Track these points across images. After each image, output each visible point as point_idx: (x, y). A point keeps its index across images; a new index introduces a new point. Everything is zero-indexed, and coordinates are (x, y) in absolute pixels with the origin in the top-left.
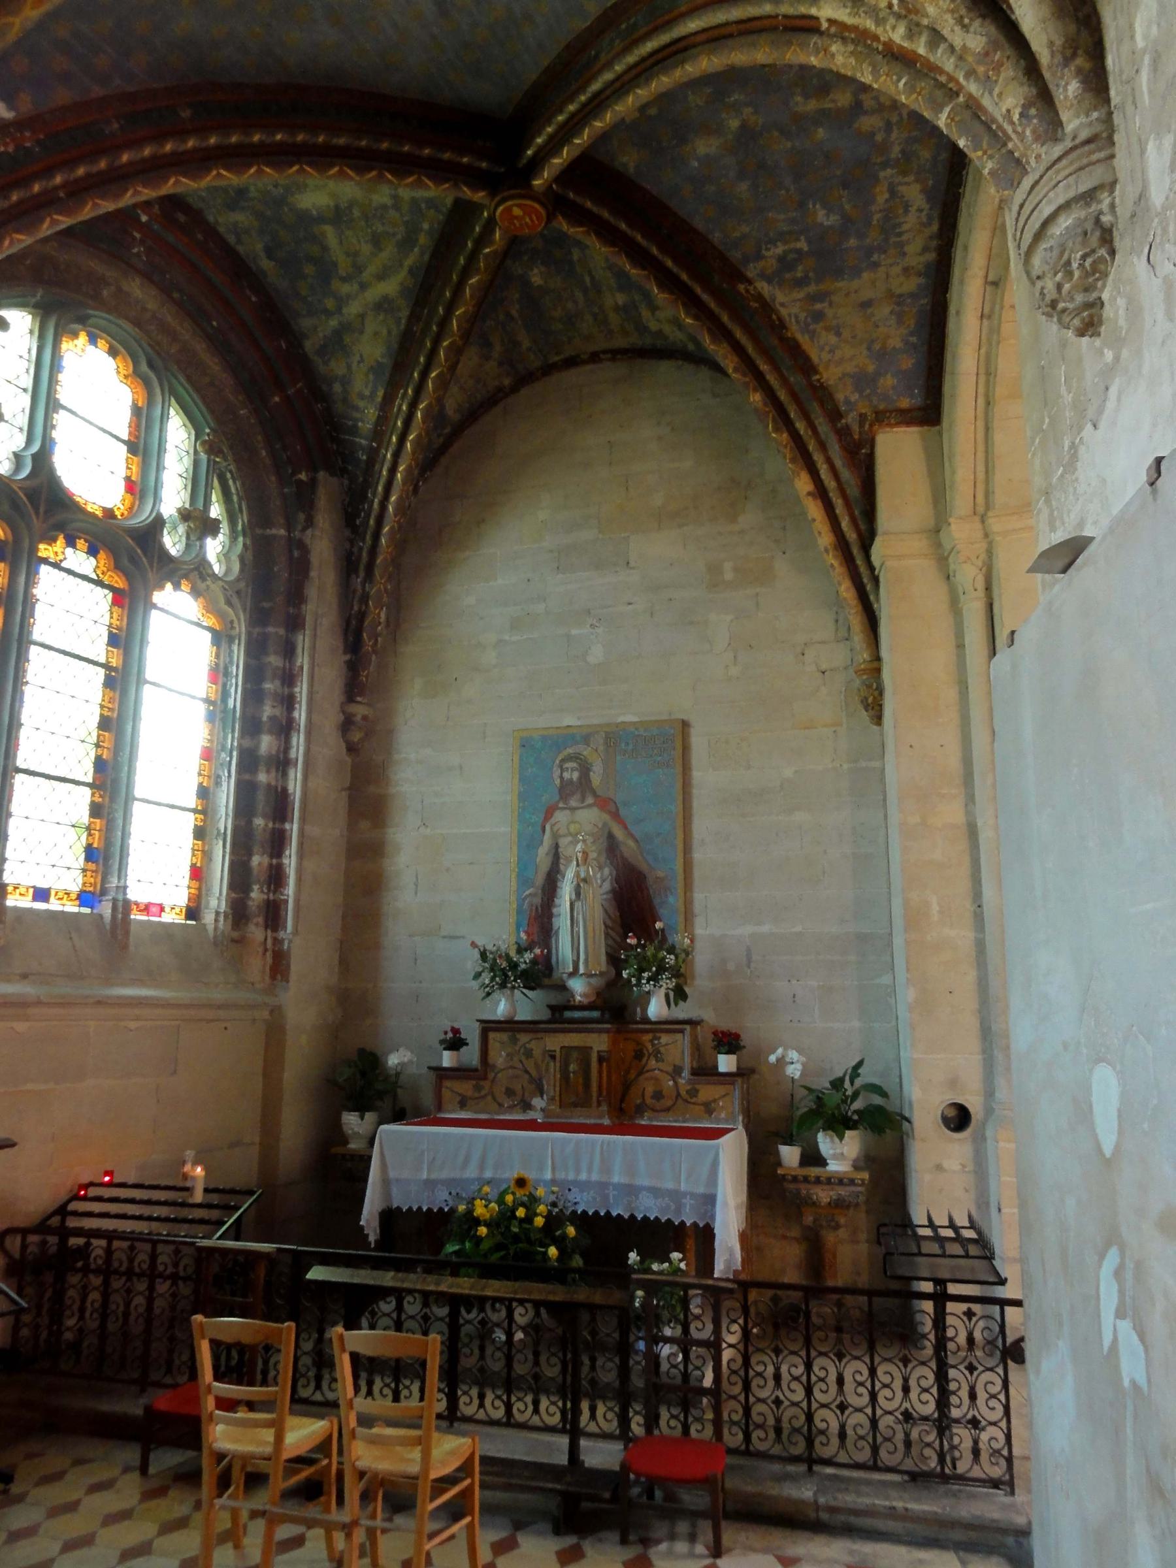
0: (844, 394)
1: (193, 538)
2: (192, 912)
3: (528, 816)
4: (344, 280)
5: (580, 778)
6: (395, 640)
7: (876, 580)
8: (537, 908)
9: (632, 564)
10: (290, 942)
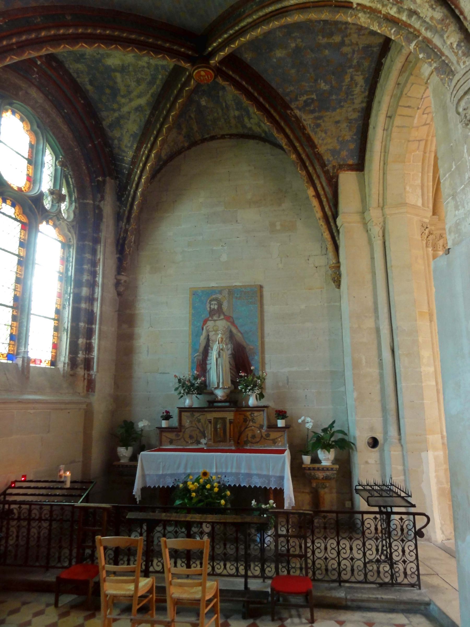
0: (327, 157)
1: (55, 202)
2: (53, 363)
3: (196, 323)
4: (123, 97)
5: (218, 308)
6: (138, 250)
7: (338, 231)
8: (200, 362)
9: (239, 221)
10: (95, 375)
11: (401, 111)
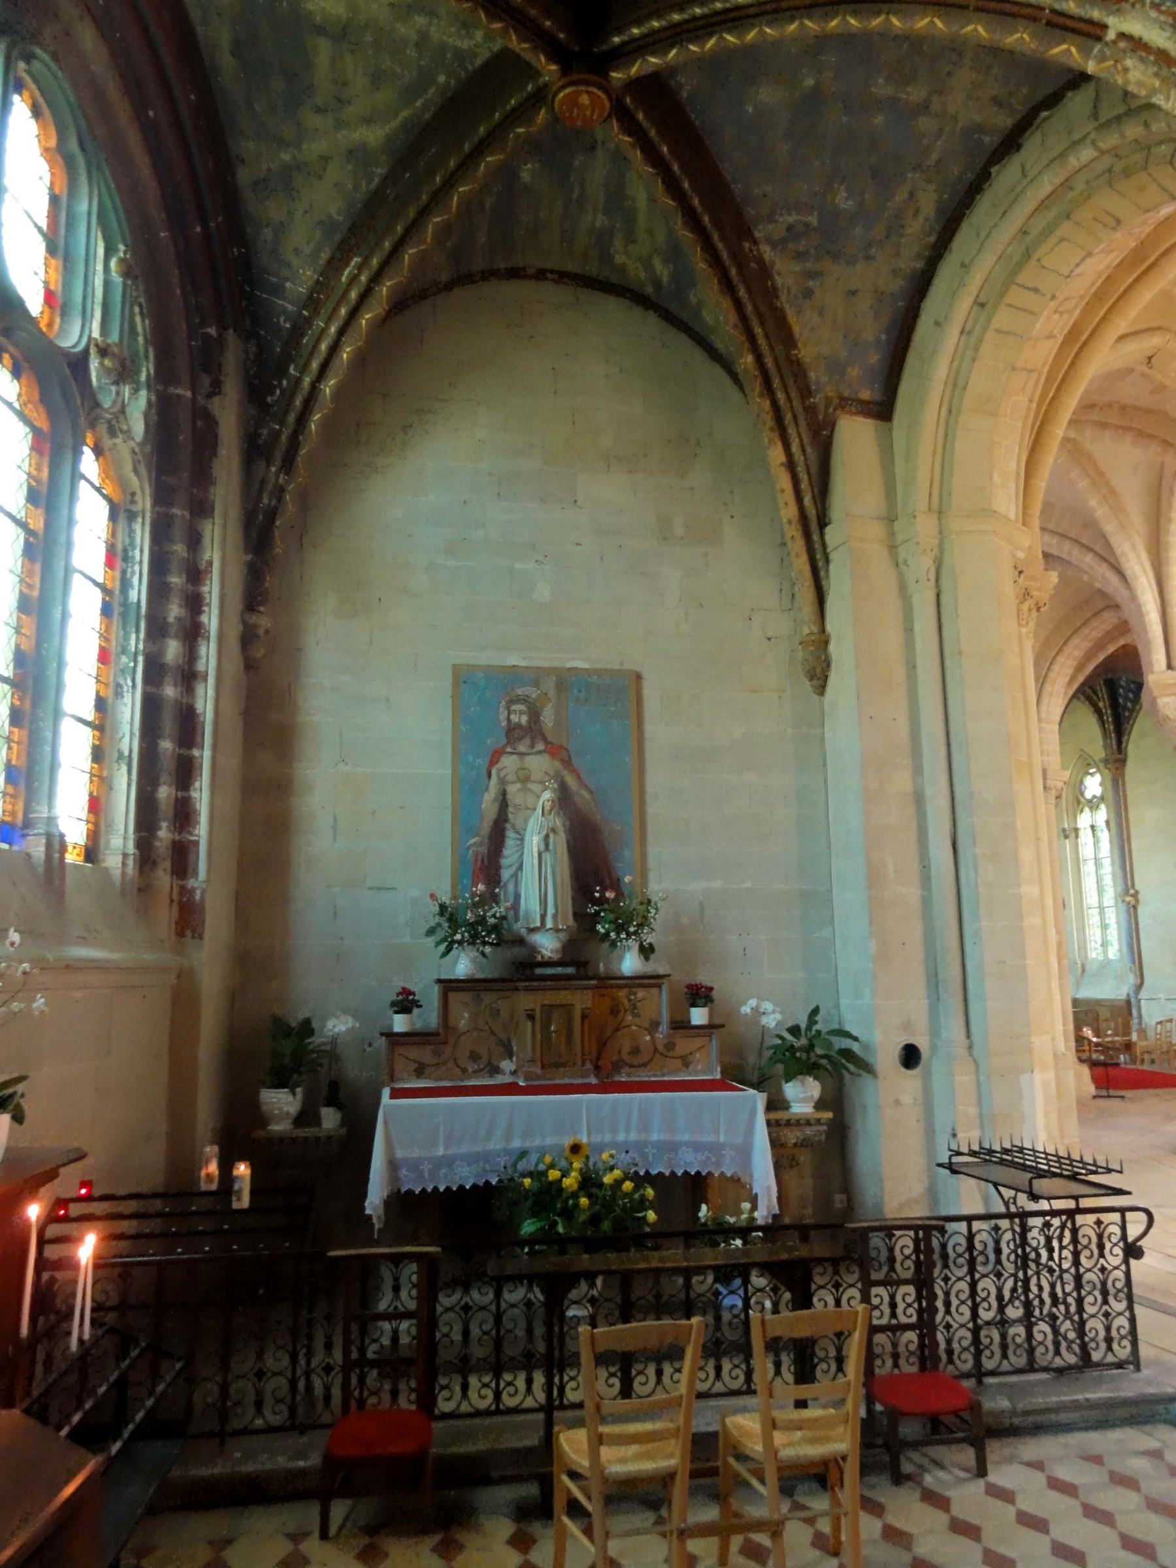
4: (319, 110)
5: (529, 722)
8: (483, 859)
9: (580, 503)
10: (203, 892)
11: (1015, 296)
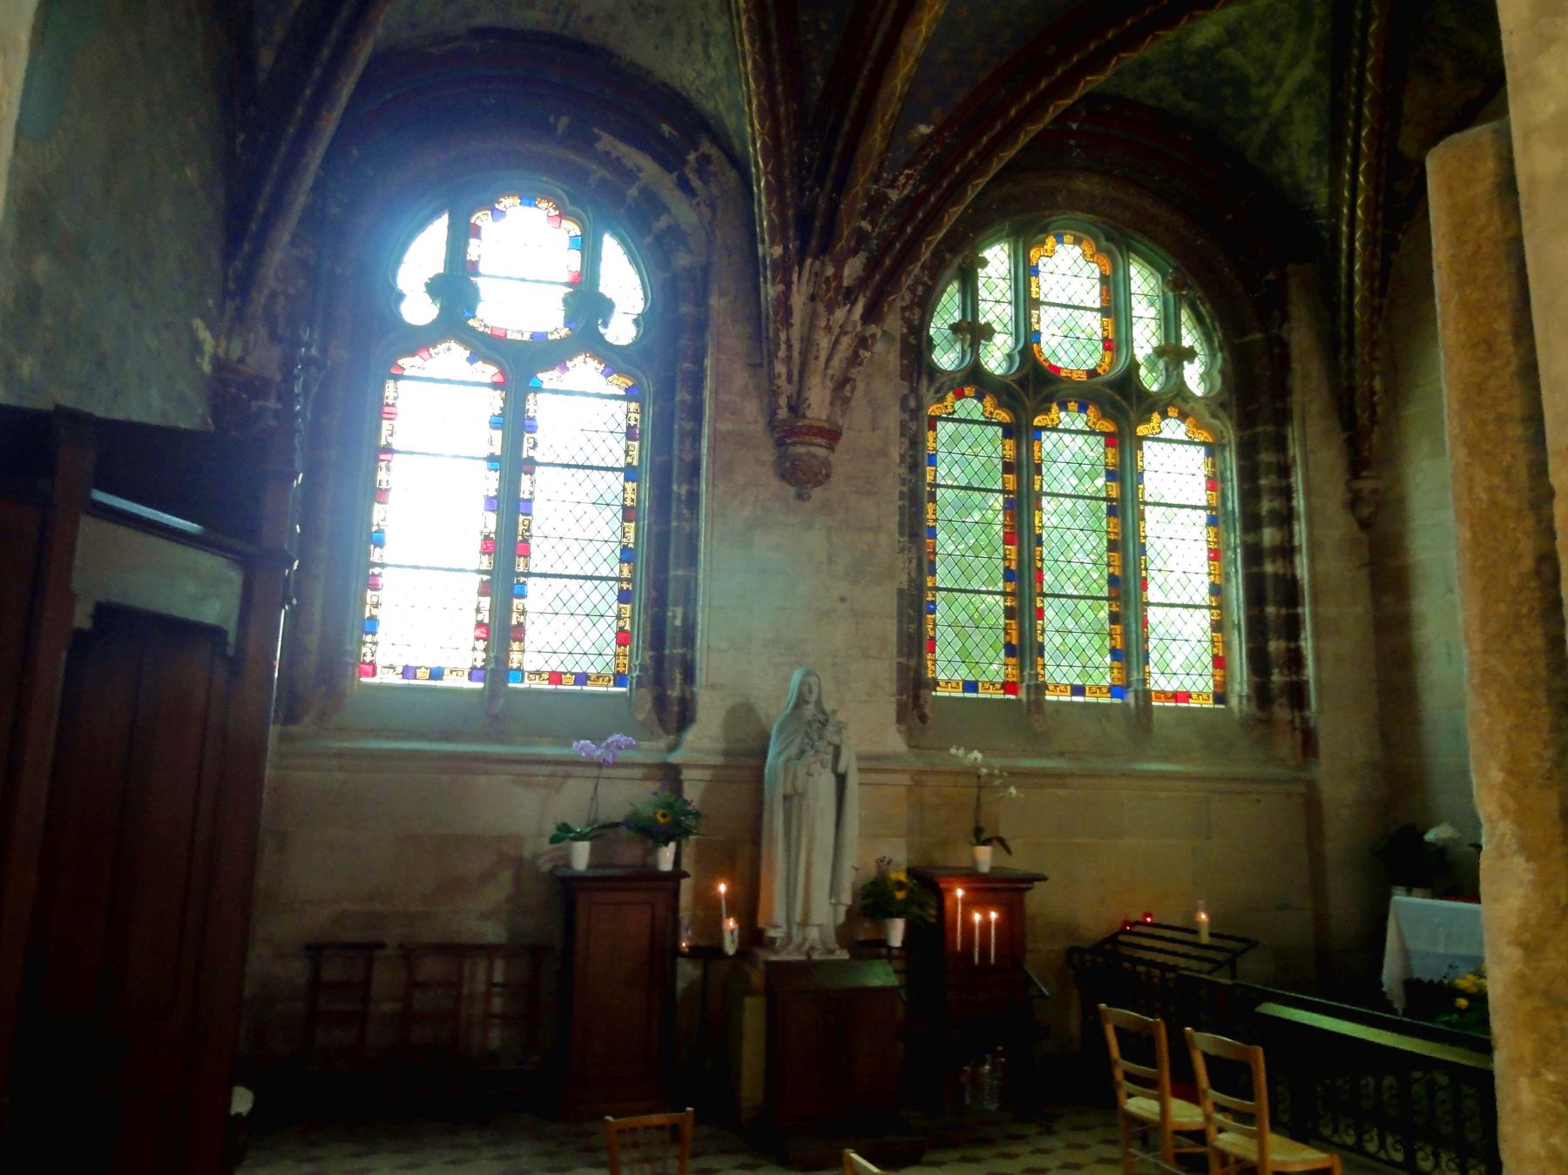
1: (1171, 369)
2: (1220, 698)
4: (1262, 83)
